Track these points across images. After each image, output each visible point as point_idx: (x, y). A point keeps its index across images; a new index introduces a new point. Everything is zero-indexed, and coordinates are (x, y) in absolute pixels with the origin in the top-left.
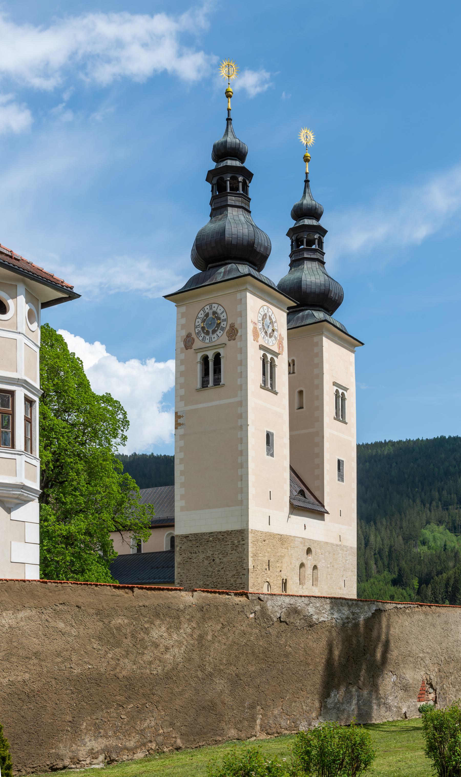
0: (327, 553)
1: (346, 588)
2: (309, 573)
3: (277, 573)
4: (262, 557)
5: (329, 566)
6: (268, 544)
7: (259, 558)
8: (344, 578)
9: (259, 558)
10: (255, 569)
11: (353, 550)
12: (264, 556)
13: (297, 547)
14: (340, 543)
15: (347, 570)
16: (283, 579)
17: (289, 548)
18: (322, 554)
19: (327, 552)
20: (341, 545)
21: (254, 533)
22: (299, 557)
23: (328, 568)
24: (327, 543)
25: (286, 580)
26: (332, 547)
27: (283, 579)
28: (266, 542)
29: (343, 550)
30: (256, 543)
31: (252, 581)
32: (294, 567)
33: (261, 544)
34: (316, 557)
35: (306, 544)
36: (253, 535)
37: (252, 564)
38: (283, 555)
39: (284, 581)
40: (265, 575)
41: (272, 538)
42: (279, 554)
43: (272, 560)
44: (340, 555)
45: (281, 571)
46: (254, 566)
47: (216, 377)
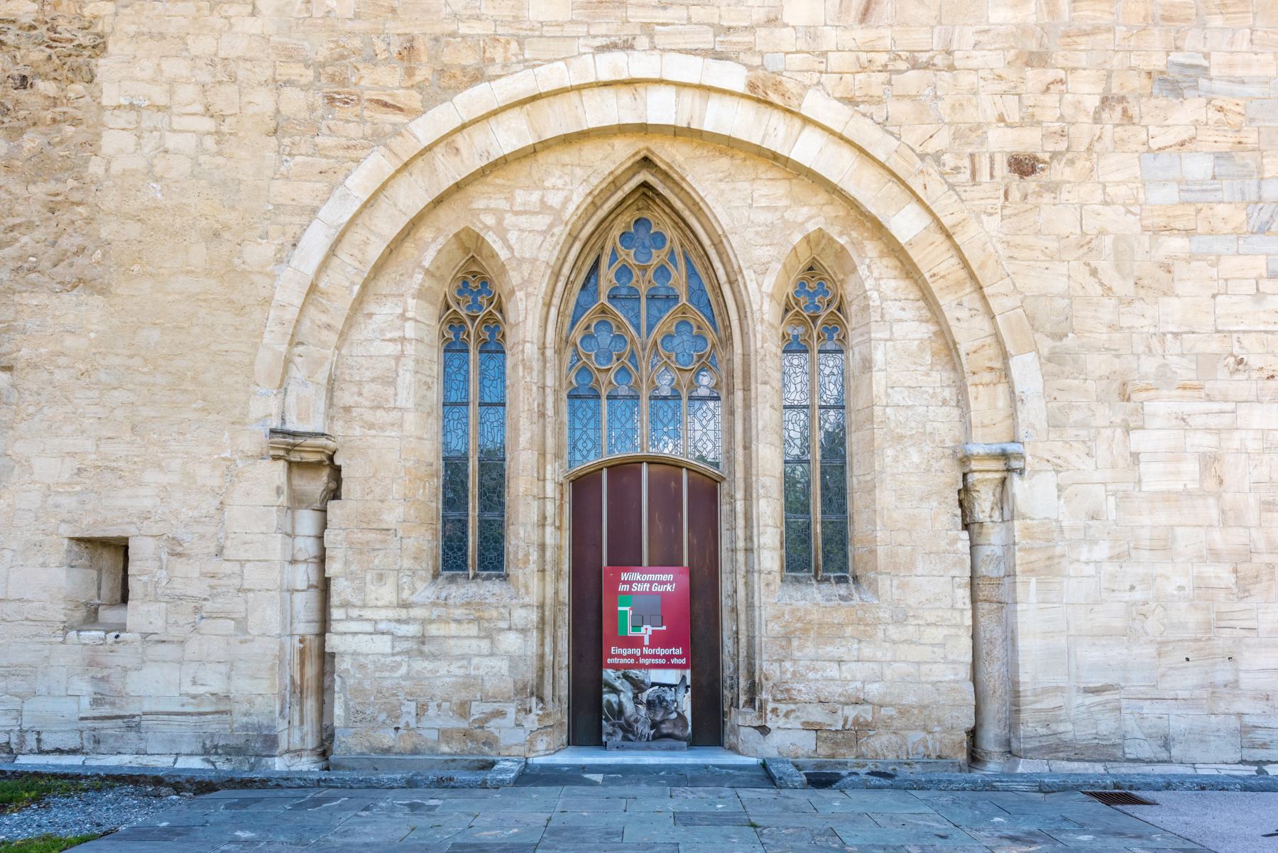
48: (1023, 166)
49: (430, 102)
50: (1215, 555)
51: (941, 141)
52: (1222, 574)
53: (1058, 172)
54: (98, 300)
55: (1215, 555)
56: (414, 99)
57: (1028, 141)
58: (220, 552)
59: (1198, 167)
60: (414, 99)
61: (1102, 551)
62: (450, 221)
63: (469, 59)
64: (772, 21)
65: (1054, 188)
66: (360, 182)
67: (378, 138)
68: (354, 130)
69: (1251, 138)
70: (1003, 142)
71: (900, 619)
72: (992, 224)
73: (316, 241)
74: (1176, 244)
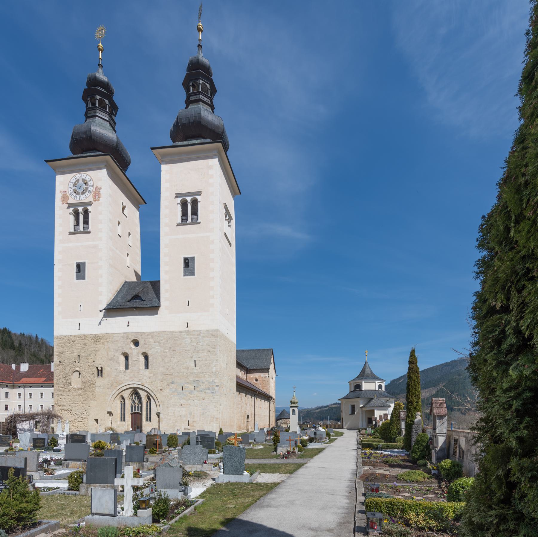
0: (164, 340)
1: (197, 368)
2: (135, 360)
3: (89, 364)
4: (71, 353)
5: (167, 351)
6: (77, 344)
7: (66, 355)
8: (194, 359)
9: (66, 355)
10: (61, 364)
11: (210, 333)
12: (73, 353)
13: (117, 341)
14: (187, 329)
15: (200, 351)
16: (97, 368)
17: (106, 343)
18: (155, 342)
19: (164, 339)
20: (188, 331)
21: (60, 338)
22: (120, 348)
23: (166, 352)
24: (163, 332)
25: (102, 368)
26: (173, 334)
27: (97, 368)
28: (76, 342)
29: (194, 335)
30: (63, 345)
31: (58, 372)
32: (112, 356)
33: (68, 345)
34: (146, 345)
35: (130, 337)
36: (59, 339)
37: (58, 360)
38: (97, 349)
39: (100, 369)
40: (74, 366)
41: (82, 338)
42: (92, 349)
43: (82, 354)
44: (187, 339)
45: (94, 362)
46: (60, 362)
47: (85, 226)
48: (161, 390)
49: (119, 386)
50: (174, 420)
51: (155, 388)
52: (174, 421)
53: (163, 390)
54: (96, 401)
55: (174, 420)
56: (117, 386)
57: (161, 388)
58: (104, 420)
59: (174, 390)
60: (117, 386)
61: (166, 420)
62: (120, 394)
63: (121, 382)
64: (143, 379)
65: (163, 391)
66: (114, 392)
67: (115, 389)
68: (113, 388)
69: (178, 387)
70: (160, 388)
71: (153, 425)
72: (158, 394)
73: (111, 397)
74: (172, 396)
